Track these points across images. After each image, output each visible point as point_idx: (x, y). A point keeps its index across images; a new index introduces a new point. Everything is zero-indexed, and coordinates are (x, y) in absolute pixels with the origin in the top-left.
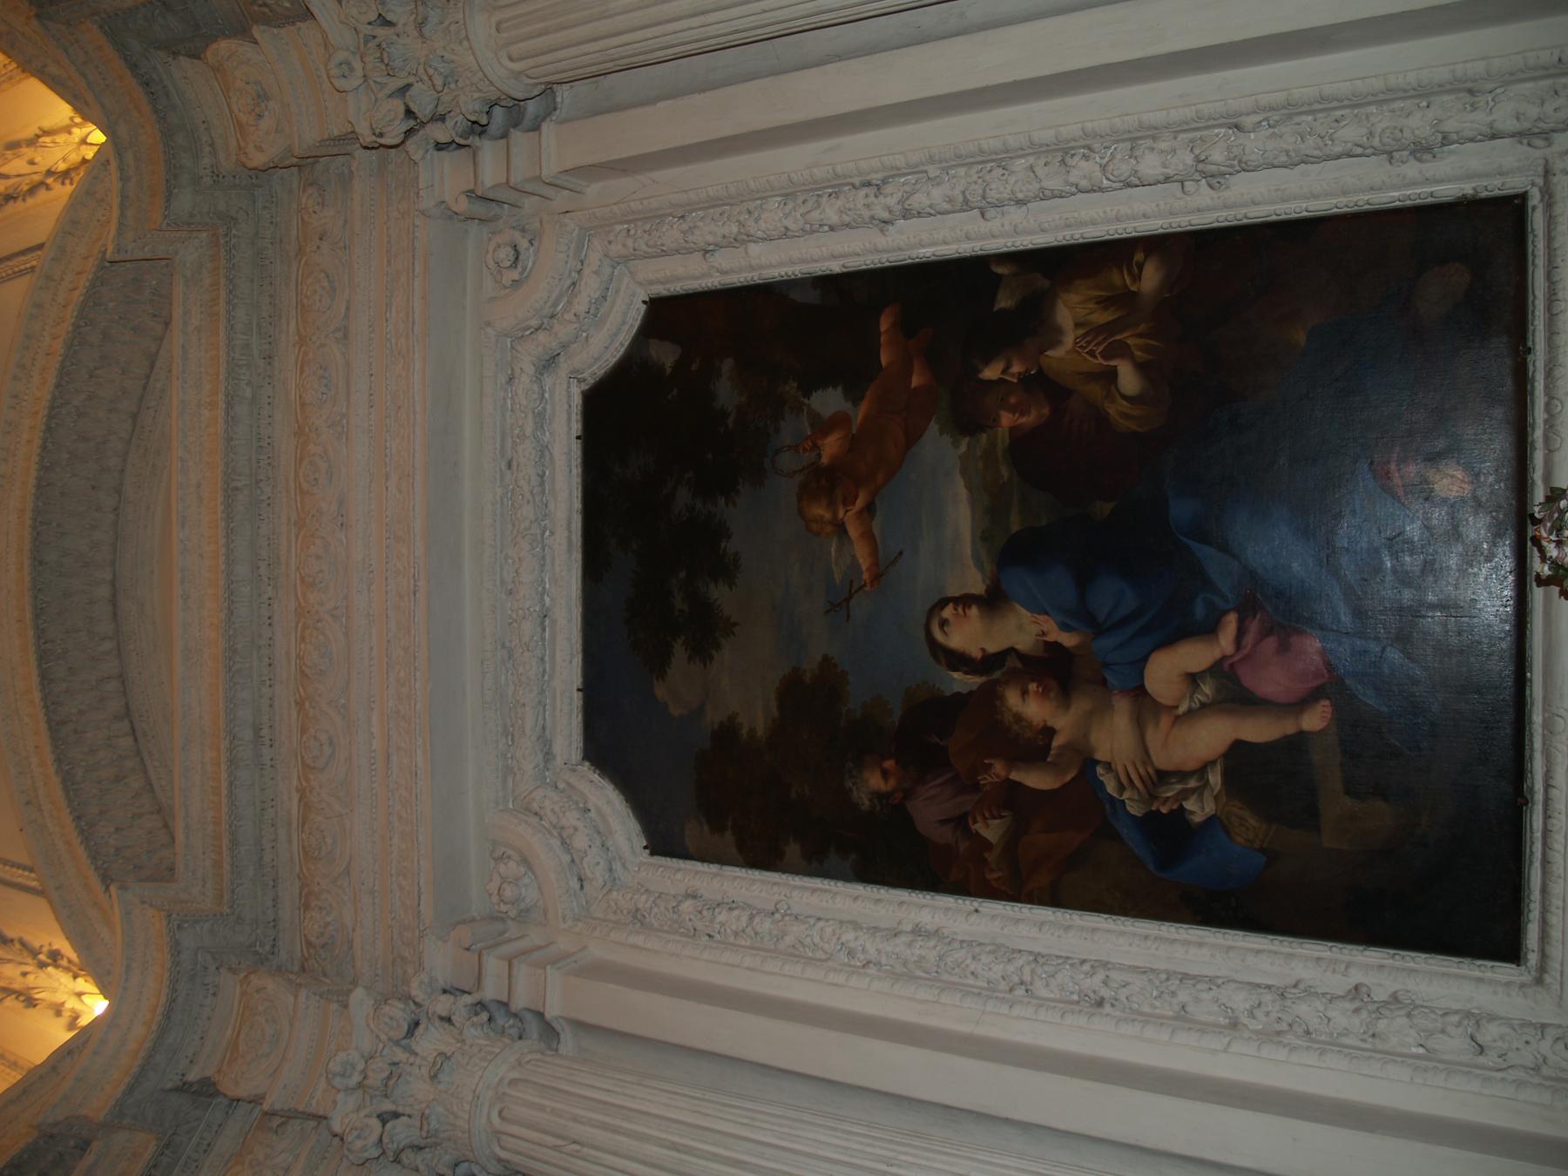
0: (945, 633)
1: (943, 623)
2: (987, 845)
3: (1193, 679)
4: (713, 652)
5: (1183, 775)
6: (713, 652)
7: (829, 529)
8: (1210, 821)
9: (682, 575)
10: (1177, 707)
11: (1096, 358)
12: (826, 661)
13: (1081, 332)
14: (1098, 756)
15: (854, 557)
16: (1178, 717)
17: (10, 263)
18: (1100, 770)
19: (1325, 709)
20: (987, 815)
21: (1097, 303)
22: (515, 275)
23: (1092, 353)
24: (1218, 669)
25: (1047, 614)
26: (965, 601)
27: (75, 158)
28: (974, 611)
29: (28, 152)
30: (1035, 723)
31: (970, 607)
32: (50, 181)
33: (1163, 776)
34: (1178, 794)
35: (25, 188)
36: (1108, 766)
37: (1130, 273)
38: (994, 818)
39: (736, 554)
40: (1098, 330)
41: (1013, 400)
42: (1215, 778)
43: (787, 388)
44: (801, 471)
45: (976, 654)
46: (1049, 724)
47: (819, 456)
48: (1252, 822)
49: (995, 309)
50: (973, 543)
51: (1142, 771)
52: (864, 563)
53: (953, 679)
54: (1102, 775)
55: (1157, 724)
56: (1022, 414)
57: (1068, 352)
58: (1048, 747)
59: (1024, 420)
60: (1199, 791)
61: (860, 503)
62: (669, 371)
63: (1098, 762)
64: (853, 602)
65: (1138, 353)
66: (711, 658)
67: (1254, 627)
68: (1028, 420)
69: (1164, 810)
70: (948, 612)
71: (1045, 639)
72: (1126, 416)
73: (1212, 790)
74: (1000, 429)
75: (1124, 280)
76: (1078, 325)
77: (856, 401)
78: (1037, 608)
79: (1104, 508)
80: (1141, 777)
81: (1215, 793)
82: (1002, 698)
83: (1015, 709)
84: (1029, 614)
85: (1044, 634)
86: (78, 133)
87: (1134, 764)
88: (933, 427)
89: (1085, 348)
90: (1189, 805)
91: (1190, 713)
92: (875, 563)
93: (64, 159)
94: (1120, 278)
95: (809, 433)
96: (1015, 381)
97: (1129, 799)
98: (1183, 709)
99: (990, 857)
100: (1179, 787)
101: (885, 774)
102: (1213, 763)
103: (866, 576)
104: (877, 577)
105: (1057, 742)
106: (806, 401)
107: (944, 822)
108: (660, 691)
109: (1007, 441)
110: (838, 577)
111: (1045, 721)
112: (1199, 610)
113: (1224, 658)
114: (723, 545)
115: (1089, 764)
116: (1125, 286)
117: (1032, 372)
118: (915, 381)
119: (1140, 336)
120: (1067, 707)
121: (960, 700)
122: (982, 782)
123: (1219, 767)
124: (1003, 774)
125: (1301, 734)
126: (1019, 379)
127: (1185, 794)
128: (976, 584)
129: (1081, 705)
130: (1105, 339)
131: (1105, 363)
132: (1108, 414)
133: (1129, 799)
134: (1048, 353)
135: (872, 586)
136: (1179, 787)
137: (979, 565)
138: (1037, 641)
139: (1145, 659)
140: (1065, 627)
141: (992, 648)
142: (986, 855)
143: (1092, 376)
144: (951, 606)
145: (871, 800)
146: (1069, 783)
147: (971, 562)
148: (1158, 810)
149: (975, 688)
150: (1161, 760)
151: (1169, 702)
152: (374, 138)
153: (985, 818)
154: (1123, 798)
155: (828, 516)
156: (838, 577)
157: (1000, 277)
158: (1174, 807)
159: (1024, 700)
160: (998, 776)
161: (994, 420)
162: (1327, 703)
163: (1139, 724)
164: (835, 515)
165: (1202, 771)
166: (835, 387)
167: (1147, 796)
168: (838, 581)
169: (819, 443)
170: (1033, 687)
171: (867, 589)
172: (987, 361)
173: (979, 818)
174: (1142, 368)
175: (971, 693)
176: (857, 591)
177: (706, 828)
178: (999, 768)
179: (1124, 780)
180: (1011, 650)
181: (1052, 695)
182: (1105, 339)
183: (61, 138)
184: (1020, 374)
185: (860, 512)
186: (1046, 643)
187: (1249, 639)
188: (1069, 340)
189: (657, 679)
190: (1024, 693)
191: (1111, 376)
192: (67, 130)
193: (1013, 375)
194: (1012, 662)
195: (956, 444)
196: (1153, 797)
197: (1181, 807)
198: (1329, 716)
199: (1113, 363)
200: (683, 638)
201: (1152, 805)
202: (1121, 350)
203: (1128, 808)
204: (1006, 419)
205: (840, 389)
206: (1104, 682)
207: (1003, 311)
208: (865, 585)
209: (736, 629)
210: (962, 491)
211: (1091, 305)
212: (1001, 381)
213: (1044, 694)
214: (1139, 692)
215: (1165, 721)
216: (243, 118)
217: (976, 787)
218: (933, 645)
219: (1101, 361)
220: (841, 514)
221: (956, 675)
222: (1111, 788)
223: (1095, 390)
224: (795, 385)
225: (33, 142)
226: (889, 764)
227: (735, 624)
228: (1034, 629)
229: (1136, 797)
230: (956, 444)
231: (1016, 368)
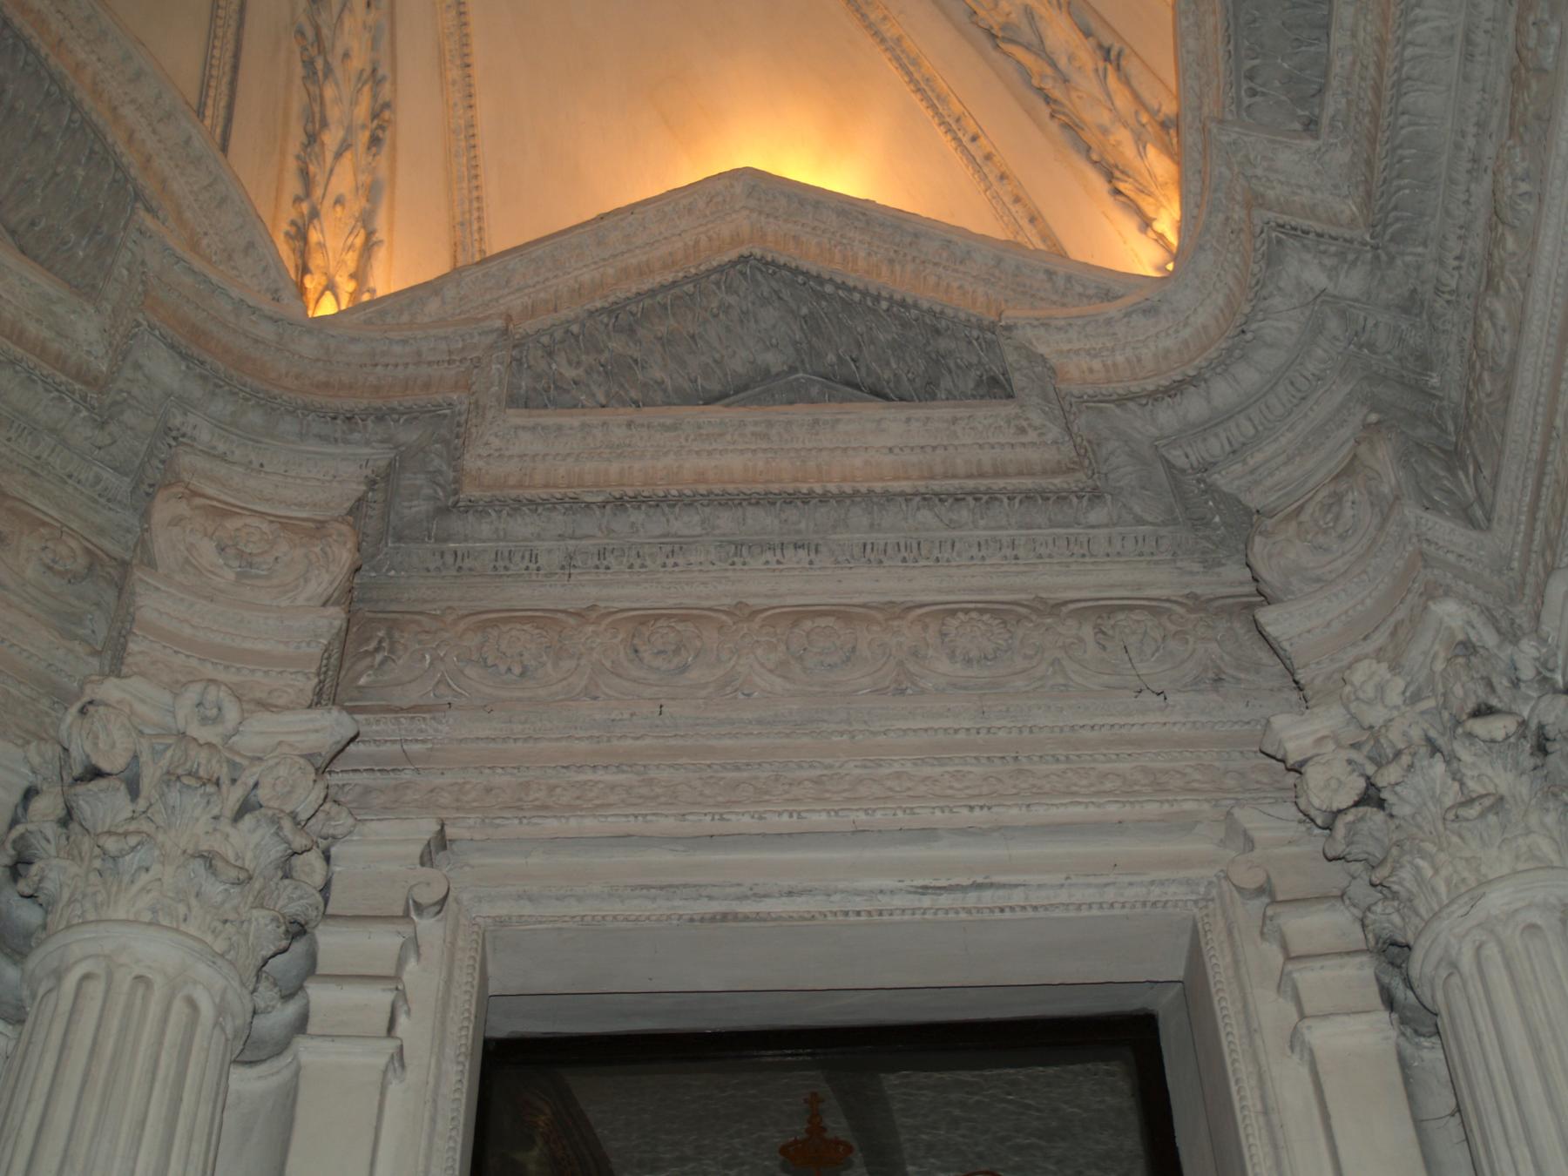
17: (226, 80)
27: (316, 261)
29: (356, 205)
32: (305, 207)
35: (312, 168)
86: (347, 286)
93: (322, 246)
152: (86, 699)
183: (351, 259)
192: (359, 276)
216: (231, 524)
225: (366, 221)
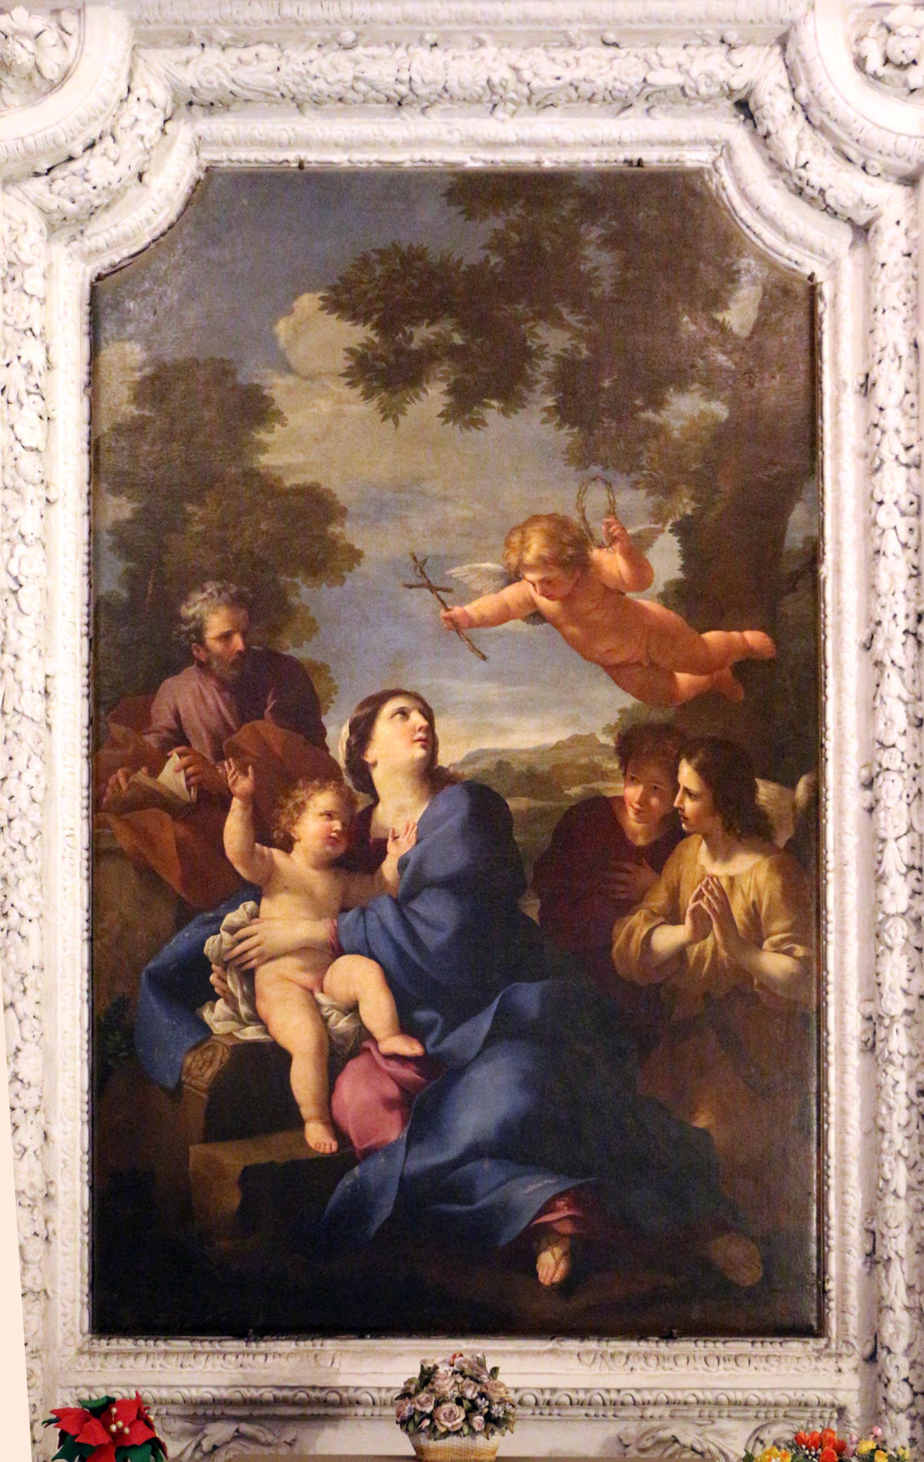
0: (393, 716)
1: (404, 713)
2: (155, 771)
3: (353, 1009)
4: (360, 389)
5: (251, 998)
6: (360, 389)
7: (513, 559)
8: (206, 1029)
9: (457, 339)
10: (322, 991)
11: (695, 900)
12: (355, 555)
13: (724, 883)
14: (265, 902)
15: (479, 594)
16: (311, 992)
18: (250, 905)
19: (328, 1147)
20: (190, 770)
21: (754, 903)
22: (874, 63)
23: (700, 896)
24: (364, 1035)
25: (418, 842)
26: (430, 742)
28: (419, 752)
30: (296, 828)
31: (424, 747)
33: (248, 977)
34: (231, 994)
36: (254, 915)
37: (783, 941)
38: (187, 779)
39: (485, 424)
40: (724, 903)
41: (654, 801)
42: (251, 1033)
43: (685, 500)
44: (584, 518)
45: (371, 756)
46: (297, 846)
47: (601, 547)
48: (209, 1073)
49: (757, 780)
50: (495, 752)
51: (253, 953)
52: (476, 608)
53: (341, 726)
54: (245, 907)
55: (304, 969)
56: (638, 812)
57: (703, 867)
58: (271, 844)
59: (631, 814)
60: (235, 1016)
61: (544, 603)
62: (719, 317)
63: (258, 903)
64: (427, 591)
65: (696, 948)
66: (352, 385)
67: (408, 1073)
68: (632, 822)
69: (213, 978)
70: (417, 719)
71: (390, 839)
72: (629, 936)
73: (238, 1030)
74: (622, 785)
75: (776, 933)
76: (732, 879)
77: (664, 598)
78: (424, 828)
79: (532, 908)
80: (245, 952)
81: (235, 1034)
82: (322, 788)
83: (310, 804)
84: (416, 820)
85: (395, 838)
87: (258, 945)
88: (628, 701)
89: (707, 889)
90: (220, 1005)
91: (317, 1006)
92: (472, 624)
94: (778, 928)
95: (629, 531)
96: (675, 804)
97: (221, 941)
98: (321, 998)
99: (142, 775)
100: (238, 994)
101: (226, 637)
102: (266, 1031)
103: (457, 611)
104: (456, 626)
105: (277, 855)
106: (668, 527)
107: (177, 717)
108: (308, 302)
109: (609, 794)
110: (457, 572)
111: (299, 840)
112: (423, 1015)
113: (376, 1042)
114: (495, 403)
115: (256, 892)
116: (770, 935)
117: (684, 826)
118: (683, 678)
119: (715, 952)
120: (316, 867)
121: (317, 734)
122: (226, 764)
123: (262, 1037)
124: (237, 789)
125: (300, 1123)
126: (677, 809)
127: (231, 1001)
128: (448, 757)
129: (320, 883)
130: (714, 911)
131: (688, 912)
132: (633, 914)
133: (221, 941)
134: (704, 845)
135: (446, 619)
136: (238, 994)
137: (472, 759)
138: (387, 830)
139: (372, 956)
140: (403, 864)
141: (377, 775)
142: (144, 769)
143: (675, 894)
144: (424, 723)
145: (194, 617)
146: (232, 867)
147: (474, 748)
148: (211, 972)
149: (331, 753)
150: (265, 975)
151: (327, 983)
153: (185, 768)
154: (223, 932)
155: (529, 558)
156: (457, 572)
157: (793, 785)
158: (216, 990)
159: (321, 815)
160: (234, 782)
161: (633, 778)
162: (334, 1148)
163: (303, 950)
164: (530, 568)
165: (256, 1018)
166: (683, 568)
167: (225, 959)
168: (452, 571)
169: (617, 546)
170: (337, 825)
171: (443, 613)
172: (701, 770)
173: (185, 759)
174: (681, 953)
175: (326, 749)
176: (439, 597)
177: (138, 376)
178: (243, 784)
179: (241, 933)
180: (376, 799)
181: (329, 848)
182: (714, 911)
184: (683, 810)
185: (532, 603)
186: (386, 841)
187: (393, 1067)
188: (719, 870)
189: (322, 298)
190: (329, 815)
191: (674, 917)
193: (682, 801)
194: (363, 800)
195: (608, 730)
196: (226, 966)
197: (216, 998)
198: (321, 1150)
199: (688, 920)
200: (377, 340)
201: (217, 964)
202: (700, 931)
203: (212, 938)
204: (633, 793)
205: (680, 575)
206: (344, 910)
207: (754, 789)
208: (447, 610)
209: (390, 422)
210: (552, 739)
211: (752, 897)
212: (676, 786)
213: (331, 840)
214: (336, 950)
215: (307, 979)
217: (220, 756)
218: (378, 701)
219: (691, 906)
220: (531, 576)
221: (345, 730)
222: (232, 918)
223: (659, 899)
224: (689, 512)
226: (238, 642)
227: (397, 424)
228: (400, 828)
229: (224, 947)
230: (608, 730)
231: (690, 806)
